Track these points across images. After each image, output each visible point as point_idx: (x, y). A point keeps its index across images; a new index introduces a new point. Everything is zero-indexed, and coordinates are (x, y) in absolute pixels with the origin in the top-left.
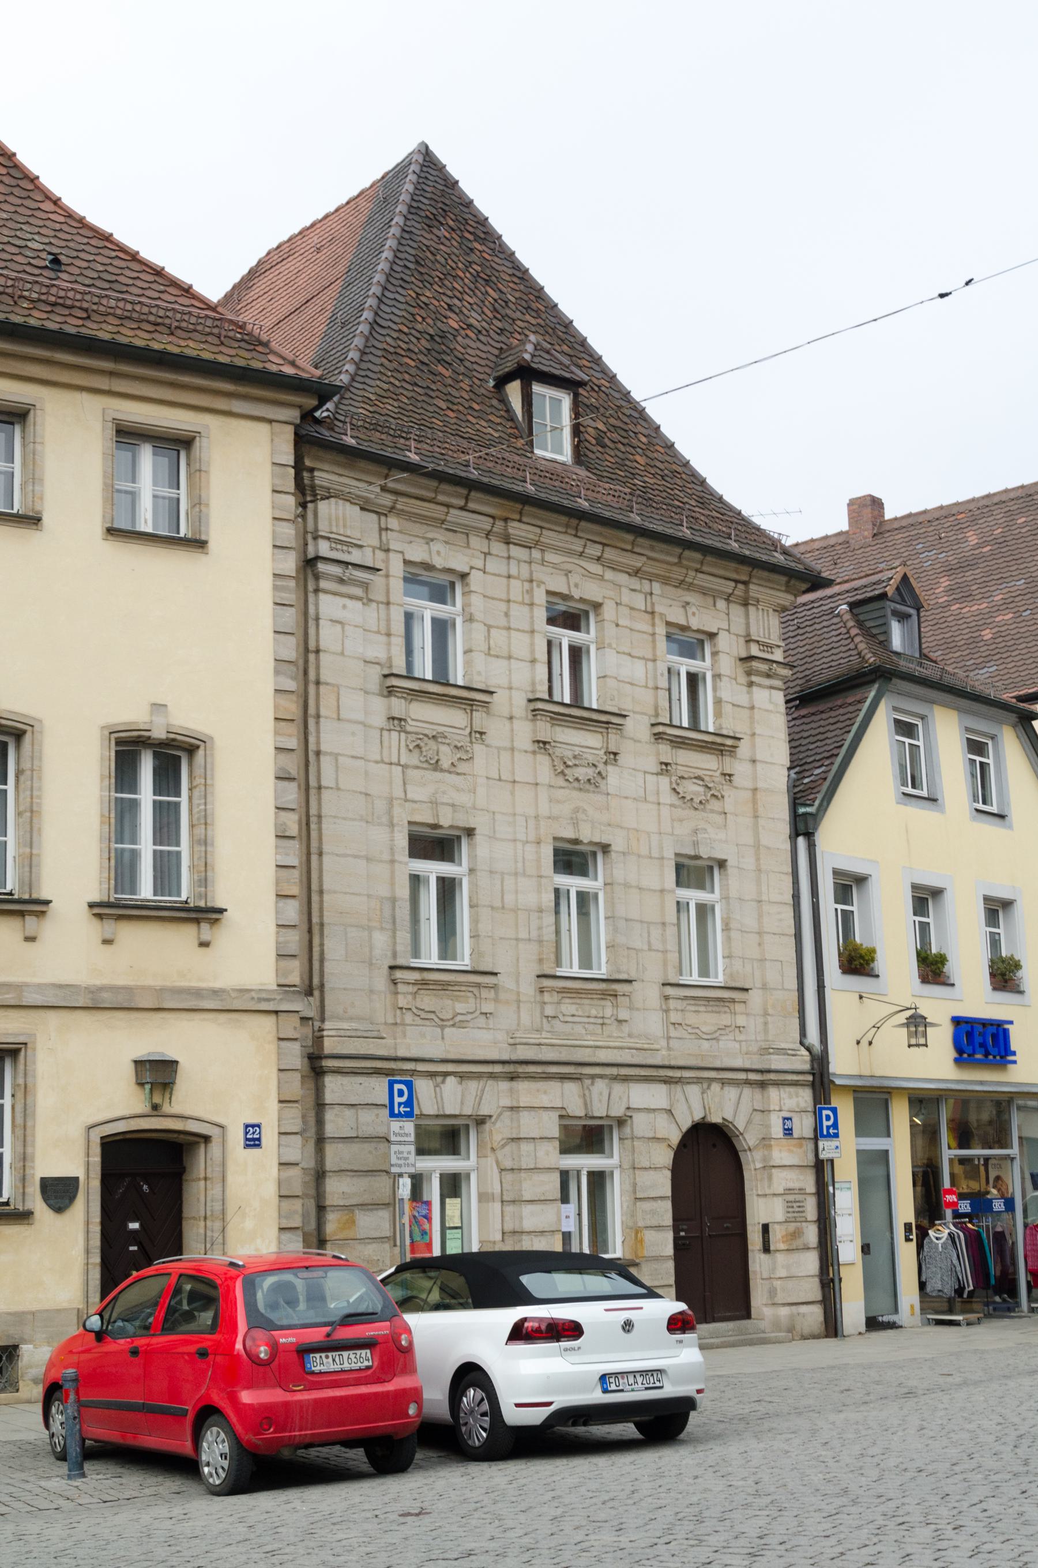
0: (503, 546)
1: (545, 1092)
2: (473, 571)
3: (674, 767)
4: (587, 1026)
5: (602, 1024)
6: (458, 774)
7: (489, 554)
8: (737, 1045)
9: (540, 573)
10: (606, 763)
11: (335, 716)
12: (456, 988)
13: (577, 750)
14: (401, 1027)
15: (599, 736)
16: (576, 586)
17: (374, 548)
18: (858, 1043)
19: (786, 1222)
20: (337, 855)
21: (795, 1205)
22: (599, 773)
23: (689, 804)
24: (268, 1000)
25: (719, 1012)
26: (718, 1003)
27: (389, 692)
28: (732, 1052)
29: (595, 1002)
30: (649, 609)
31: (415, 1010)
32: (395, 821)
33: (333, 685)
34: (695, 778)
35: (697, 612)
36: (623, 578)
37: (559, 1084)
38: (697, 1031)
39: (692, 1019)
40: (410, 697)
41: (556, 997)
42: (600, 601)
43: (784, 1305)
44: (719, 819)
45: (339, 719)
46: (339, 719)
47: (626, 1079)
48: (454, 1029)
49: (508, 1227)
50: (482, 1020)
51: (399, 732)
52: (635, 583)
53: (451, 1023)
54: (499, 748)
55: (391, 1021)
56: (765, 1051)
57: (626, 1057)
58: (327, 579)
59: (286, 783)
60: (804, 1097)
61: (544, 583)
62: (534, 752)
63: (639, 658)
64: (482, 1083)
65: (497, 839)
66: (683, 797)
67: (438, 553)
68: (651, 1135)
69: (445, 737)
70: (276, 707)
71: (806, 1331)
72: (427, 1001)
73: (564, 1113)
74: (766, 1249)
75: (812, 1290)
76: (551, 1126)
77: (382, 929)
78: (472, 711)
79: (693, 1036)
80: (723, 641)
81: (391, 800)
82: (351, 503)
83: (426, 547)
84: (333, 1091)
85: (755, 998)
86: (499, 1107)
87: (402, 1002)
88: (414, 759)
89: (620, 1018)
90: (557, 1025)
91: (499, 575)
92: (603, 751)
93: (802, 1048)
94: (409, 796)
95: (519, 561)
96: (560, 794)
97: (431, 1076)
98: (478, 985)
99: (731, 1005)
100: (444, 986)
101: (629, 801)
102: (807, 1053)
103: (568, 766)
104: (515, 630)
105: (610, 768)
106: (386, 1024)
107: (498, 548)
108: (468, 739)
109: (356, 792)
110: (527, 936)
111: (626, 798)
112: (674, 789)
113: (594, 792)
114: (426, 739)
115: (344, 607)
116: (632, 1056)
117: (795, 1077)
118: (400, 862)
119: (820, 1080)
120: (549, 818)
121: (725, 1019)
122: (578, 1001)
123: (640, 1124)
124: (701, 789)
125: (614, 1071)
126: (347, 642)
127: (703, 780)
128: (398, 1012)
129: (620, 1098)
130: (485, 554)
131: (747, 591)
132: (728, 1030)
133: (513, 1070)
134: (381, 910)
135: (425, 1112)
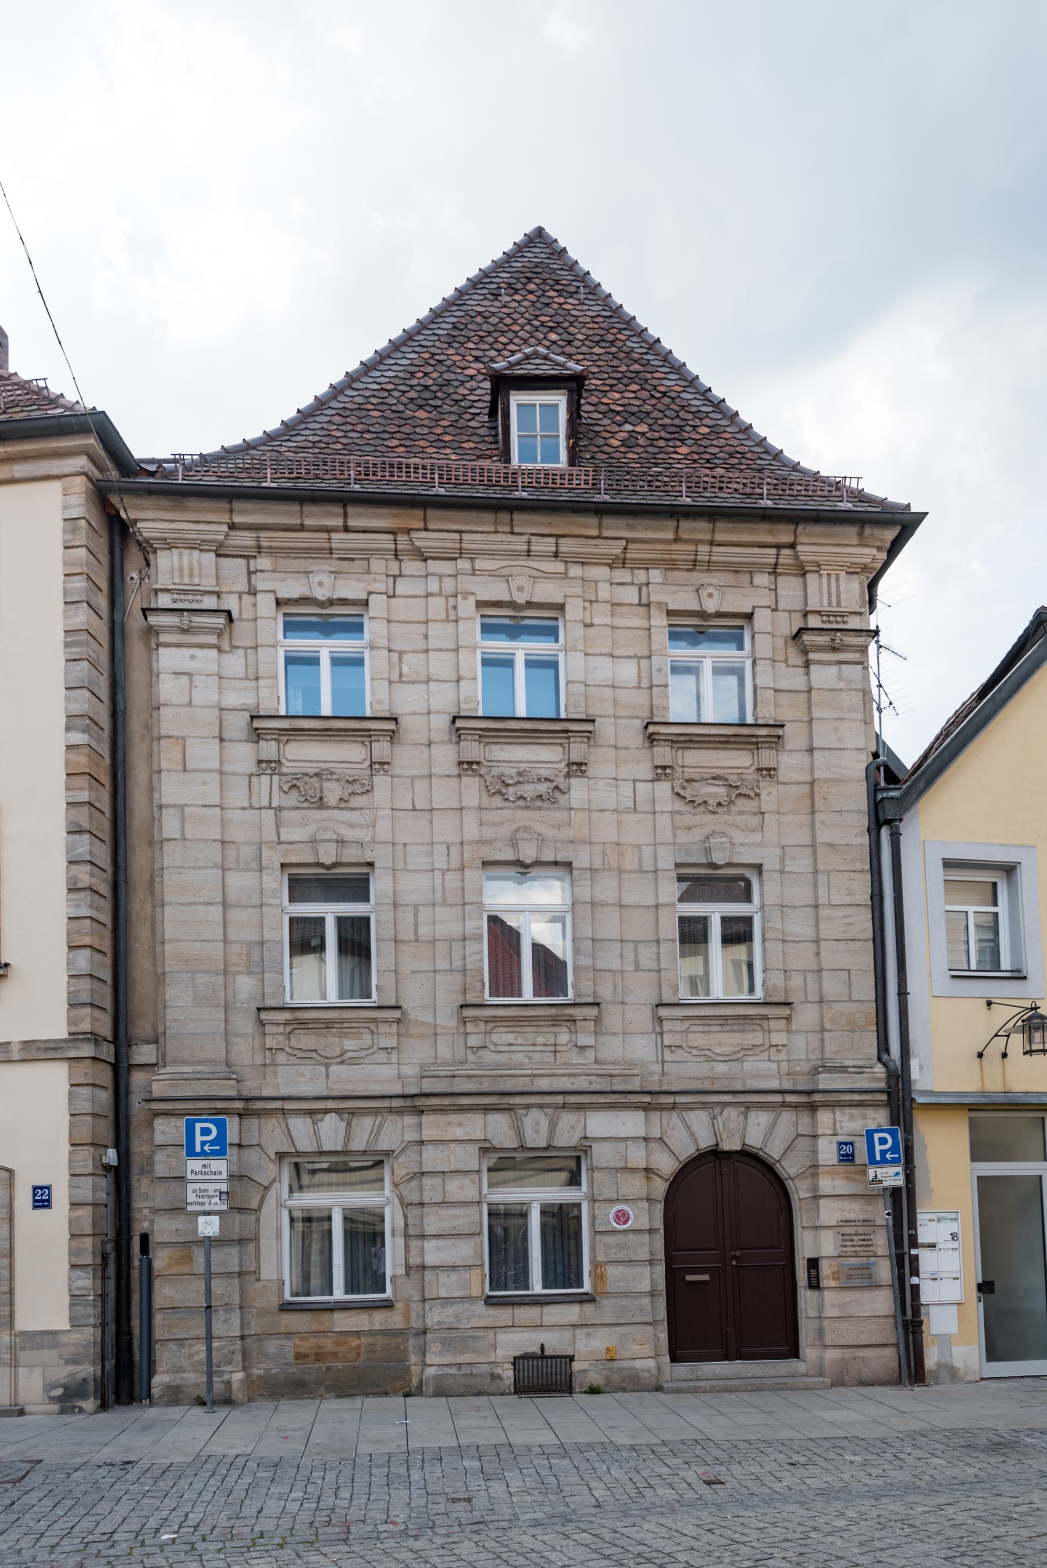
0: (423, 564)
1: (460, 1125)
2: (372, 597)
3: (680, 770)
4: (530, 1055)
5: (555, 1052)
6: (352, 809)
7: (401, 575)
8: (774, 1066)
9: (466, 583)
10: (568, 775)
11: (180, 767)
12: (345, 1025)
13: (523, 766)
14: (270, 1068)
15: (559, 749)
16: (521, 589)
17: (240, 595)
18: (980, 1055)
19: (840, 1256)
20: (182, 904)
21: (856, 1238)
22: (557, 788)
23: (702, 808)
24: (55, 1049)
25: (744, 1031)
26: (743, 1022)
27: (258, 735)
28: (763, 1072)
29: (544, 1029)
30: (644, 601)
31: (288, 1050)
32: (264, 863)
33: (178, 738)
34: (714, 778)
35: (716, 593)
36: (601, 572)
37: (482, 1116)
38: (706, 1053)
39: (698, 1039)
40: (285, 738)
41: (482, 1026)
42: (560, 601)
43: (835, 1346)
44: (754, 821)
45: (185, 770)
46: (185, 770)
47: (580, 1107)
48: (343, 1067)
49: (414, 1260)
50: (382, 1056)
51: (271, 775)
52: (622, 575)
53: (339, 1060)
54: (412, 778)
55: (259, 1062)
56: (815, 1071)
57: (582, 1084)
58: (166, 632)
59: (77, 837)
60: (879, 1118)
61: (474, 594)
62: (459, 776)
63: (628, 657)
64: (379, 1118)
65: (408, 871)
66: (693, 802)
67: (320, 584)
68: (621, 1164)
69: (332, 773)
70: (67, 763)
71: (866, 1376)
72: (305, 1040)
73: (487, 1145)
74: (815, 1284)
75: (887, 1332)
76: (468, 1157)
77: (249, 973)
78: (371, 742)
79: (702, 1059)
80: (762, 619)
81: (260, 845)
82: (201, 550)
83: (305, 581)
84: (163, 1133)
85: (806, 1016)
86: (403, 1141)
87: (270, 1042)
88: (293, 799)
89: (580, 1043)
90: (488, 1056)
91: (416, 596)
92: (563, 764)
93: (879, 1065)
94: (283, 838)
95: (441, 577)
96: (496, 816)
97: (310, 1113)
98: (375, 1021)
99: (764, 1024)
100: (328, 1024)
101: (606, 814)
102: (883, 1070)
103: (508, 785)
104: (434, 650)
105: (574, 781)
106: (254, 1065)
107: (411, 567)
108: (368, 772)
109: (209, 840)
110: (448, 967)
111: (603, 810)
112: (678, 794)
113: (549, 809)
114: (307, 778)
115: (192, 657)
116: (591, 1083)
117: (856, 1097)
118: (270, 905)
119: (899, 1099)
120: (479, 842)
121: (756, 1038)
122: (518, 1029)
123: (602, 1154)
124: (722, 790)
125: (560, 1099)
126: (195, 692)
127: (727, 780)
128: (268, 1053)
129: (572, 1127)
130: (395, 577)
131: (796, 557)
132: (757, 1050)
133: (415, 1103)
134: (249, 955)
135: (300, 1149)
